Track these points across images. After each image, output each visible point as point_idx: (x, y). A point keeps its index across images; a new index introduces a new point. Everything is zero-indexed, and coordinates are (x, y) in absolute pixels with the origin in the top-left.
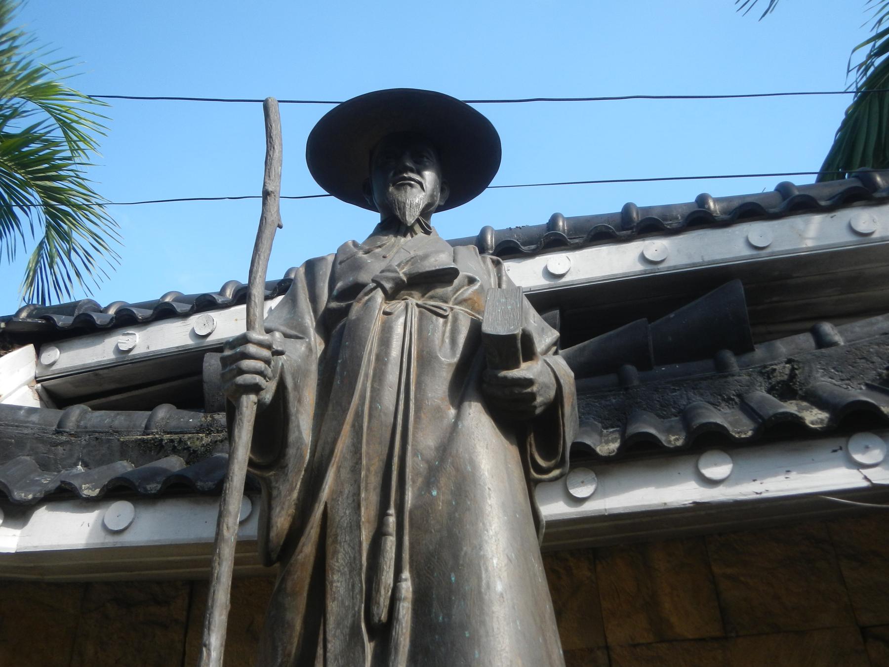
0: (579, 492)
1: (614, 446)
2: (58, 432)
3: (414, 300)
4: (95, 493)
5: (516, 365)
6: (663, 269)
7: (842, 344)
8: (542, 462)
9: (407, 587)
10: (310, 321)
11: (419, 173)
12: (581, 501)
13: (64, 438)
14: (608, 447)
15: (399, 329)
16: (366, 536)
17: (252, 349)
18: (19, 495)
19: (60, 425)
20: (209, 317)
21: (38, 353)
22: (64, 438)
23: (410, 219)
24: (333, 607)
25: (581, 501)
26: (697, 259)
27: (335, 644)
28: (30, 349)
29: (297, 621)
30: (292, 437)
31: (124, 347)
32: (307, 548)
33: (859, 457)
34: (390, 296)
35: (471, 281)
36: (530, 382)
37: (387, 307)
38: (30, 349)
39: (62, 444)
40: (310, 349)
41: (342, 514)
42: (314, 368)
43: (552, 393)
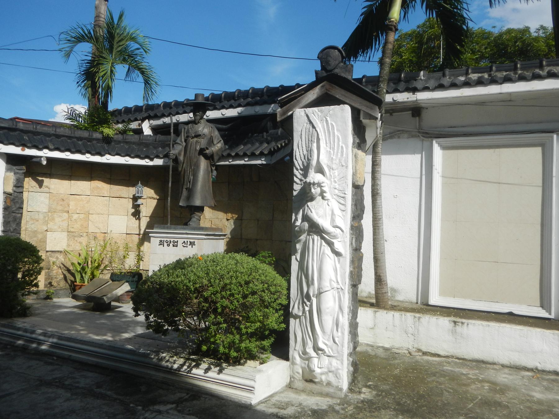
0: (230, 161)
1: (234, 154)
2: (155, 141)
3: (195, 139)
4: (162, 156)
5: (206, 151)
6: (258, 113)
7: (279, 134)
8: (212, 162)
9: (192, 178)
10: (183, 140)
11: (198, 112)
12: (230, 162)
13: (157, 143)
14: (233, 154)
15: (193, 144)
16: (188, 171)
17: (171, 154)
18: (152, 157)
19: (156, 140)
20: (179, 116)
21: (149, 121)
22: (157, 143)
23: (197, 122)
24: (185, 179)
25: (230, 162)
26: (264, 112)
27: (186, 183)
28: (147, 120)
29: (182, 180)
30: (179, 160)
31: (164, 122)
32: (182, 173)
33: (262, 159)
34: (192, 139)
35: (204, 134)
36: (207, 153)
37: (191, 140)
38: (147, 120)
39: (157, 144)
40: (182, 146)
41: (186, 169)
42: (183, 149)
43: (212, 153)
